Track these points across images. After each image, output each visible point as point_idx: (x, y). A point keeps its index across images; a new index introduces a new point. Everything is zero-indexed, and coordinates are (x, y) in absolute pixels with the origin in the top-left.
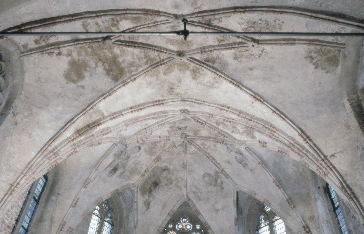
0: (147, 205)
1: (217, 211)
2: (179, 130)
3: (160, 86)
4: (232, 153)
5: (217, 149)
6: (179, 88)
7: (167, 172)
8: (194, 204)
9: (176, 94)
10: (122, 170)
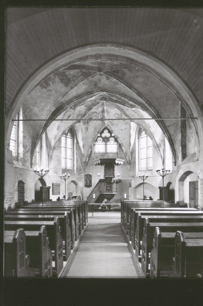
0: (87, 129)
1: (122, 130)
3: (89, 84)
8: (110, 127)
9: (98, 88)
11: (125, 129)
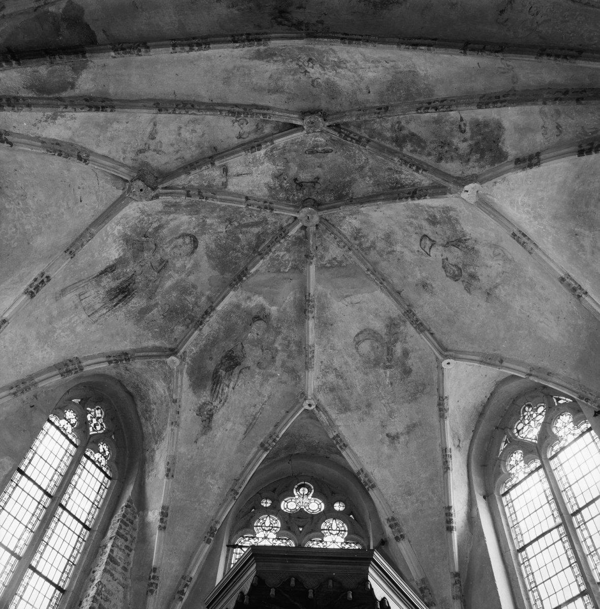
0: (206, 417)
1: (393, 438)
2: (298, 187)
4: (433, 252)
5: (393, 251)
6: (302, 10)
7: (260, 324)
10: (145, 301)
11: (408, 433)
